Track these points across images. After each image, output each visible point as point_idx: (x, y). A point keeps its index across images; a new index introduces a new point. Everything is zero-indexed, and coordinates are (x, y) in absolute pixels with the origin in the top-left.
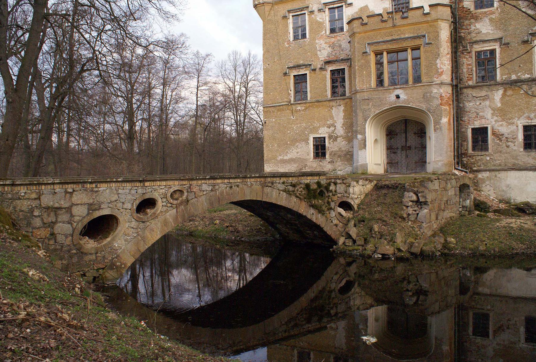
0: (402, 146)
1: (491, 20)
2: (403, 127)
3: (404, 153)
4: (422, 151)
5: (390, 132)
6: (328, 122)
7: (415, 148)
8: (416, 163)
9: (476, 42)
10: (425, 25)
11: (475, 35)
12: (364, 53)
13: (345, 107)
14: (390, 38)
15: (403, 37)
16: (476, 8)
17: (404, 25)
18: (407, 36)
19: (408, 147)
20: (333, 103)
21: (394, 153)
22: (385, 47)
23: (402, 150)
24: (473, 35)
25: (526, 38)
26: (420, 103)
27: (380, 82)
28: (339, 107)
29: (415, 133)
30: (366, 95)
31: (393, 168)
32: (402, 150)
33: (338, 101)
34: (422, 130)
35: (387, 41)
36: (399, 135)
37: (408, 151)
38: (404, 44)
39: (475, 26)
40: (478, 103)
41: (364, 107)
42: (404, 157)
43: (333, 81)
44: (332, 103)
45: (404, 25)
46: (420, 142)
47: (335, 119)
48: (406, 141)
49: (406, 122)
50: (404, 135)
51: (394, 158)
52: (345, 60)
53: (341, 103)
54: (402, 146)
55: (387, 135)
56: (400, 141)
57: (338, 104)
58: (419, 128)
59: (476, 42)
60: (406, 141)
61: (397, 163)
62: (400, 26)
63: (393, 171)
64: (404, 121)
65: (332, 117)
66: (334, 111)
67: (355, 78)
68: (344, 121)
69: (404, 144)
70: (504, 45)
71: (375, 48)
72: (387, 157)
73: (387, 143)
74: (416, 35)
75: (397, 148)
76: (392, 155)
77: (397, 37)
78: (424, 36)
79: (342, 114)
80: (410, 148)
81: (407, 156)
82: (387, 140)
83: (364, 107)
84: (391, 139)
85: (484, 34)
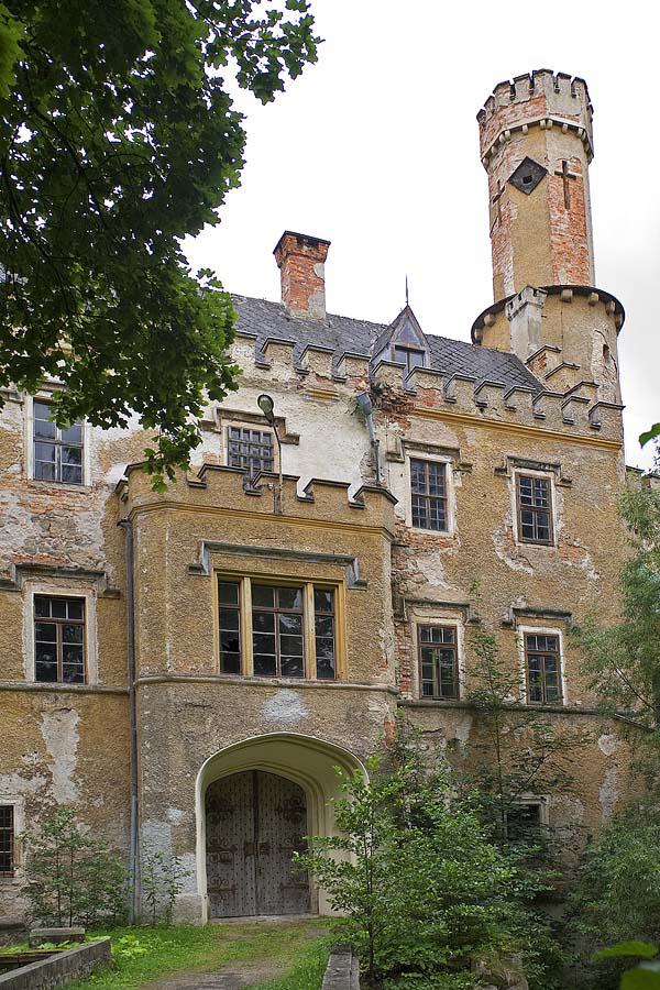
1: (445, 558)
6: (26, 760)
9: (422, 603)
10: (352, 533)
11: (415, 585)
12: (192, 568)
13: (84, 716)
14: (263, 545)
15: (297, 548)
16: (415, 522)
17: (301, 520)
18: (307, 549)
20: (47, 702)
22: (250, 565)
24: (411, 584)
25: (506, 618)
26: (341, 733)
27: (231, 663)
28: (64, 717)
30: (196, 694)
33: (61, 697)
35: (260, 552)
38: (301, 570)
39: (415, 564)
40: (423, 747)
41: (191, 727)
43: (44, 632)
44: (37, 701)
45: (301, 520)
47: (50, 751)
49: (256, 778)
52: (88, 573)
53: (71, 704)
57: (60, 706)
59: (422, 603)
62: (292, 519)
65: (39, 746)
66: (47, 727)
67: (156, 636)
68: (81, 761)
70: (471, 621)
71: (224, 560)
74: (328, 552)
77: (282, 548)
78: (350, 561)
79: (72, 739)
83: (191, 727)
85: (432, 586)
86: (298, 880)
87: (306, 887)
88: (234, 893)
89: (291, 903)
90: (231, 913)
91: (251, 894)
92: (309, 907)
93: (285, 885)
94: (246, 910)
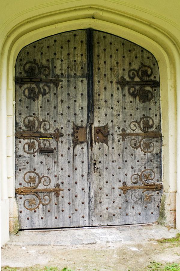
0: (76, 128)
2: (79, 55)
3: (82, 150)
4: (147, 146)
5: (32, 69)
7: (124, 135)
8: (125, 189)
19: (99, 130)
21: (46, 151)
23: (76, 143)
29: (122, 83)
31: (40, 211)
32: (76, 143)
34: (145, 73)
36: (64, 82)
37: (96, 146)
42: (82, 169)
46: (138, 115)
48: (91, 108)
50: (82, 87)
51: (42, 170)
54: (76, 128)
55: (19, 81)
56: (66, 109)
58: (136, 66)
60: (91, 108)
61: (57, 191)
63: (39, 224)
64: (83, 37)
69: (82, 118)
72: (18, 169)
73: (17, 113)
75: (58, 135)
76: (38, 158)
80: (103, 134)
81: (93, 165)
82: (18, 101)
84: (33, 96)
86: (148, 178)
87: (159, 188)
88: (57, 195)
89: (138, 209)
90: (52, 222)
91: (82, 197)
92: (162, 215)
93: (129, 184)
94: (74, 218)
